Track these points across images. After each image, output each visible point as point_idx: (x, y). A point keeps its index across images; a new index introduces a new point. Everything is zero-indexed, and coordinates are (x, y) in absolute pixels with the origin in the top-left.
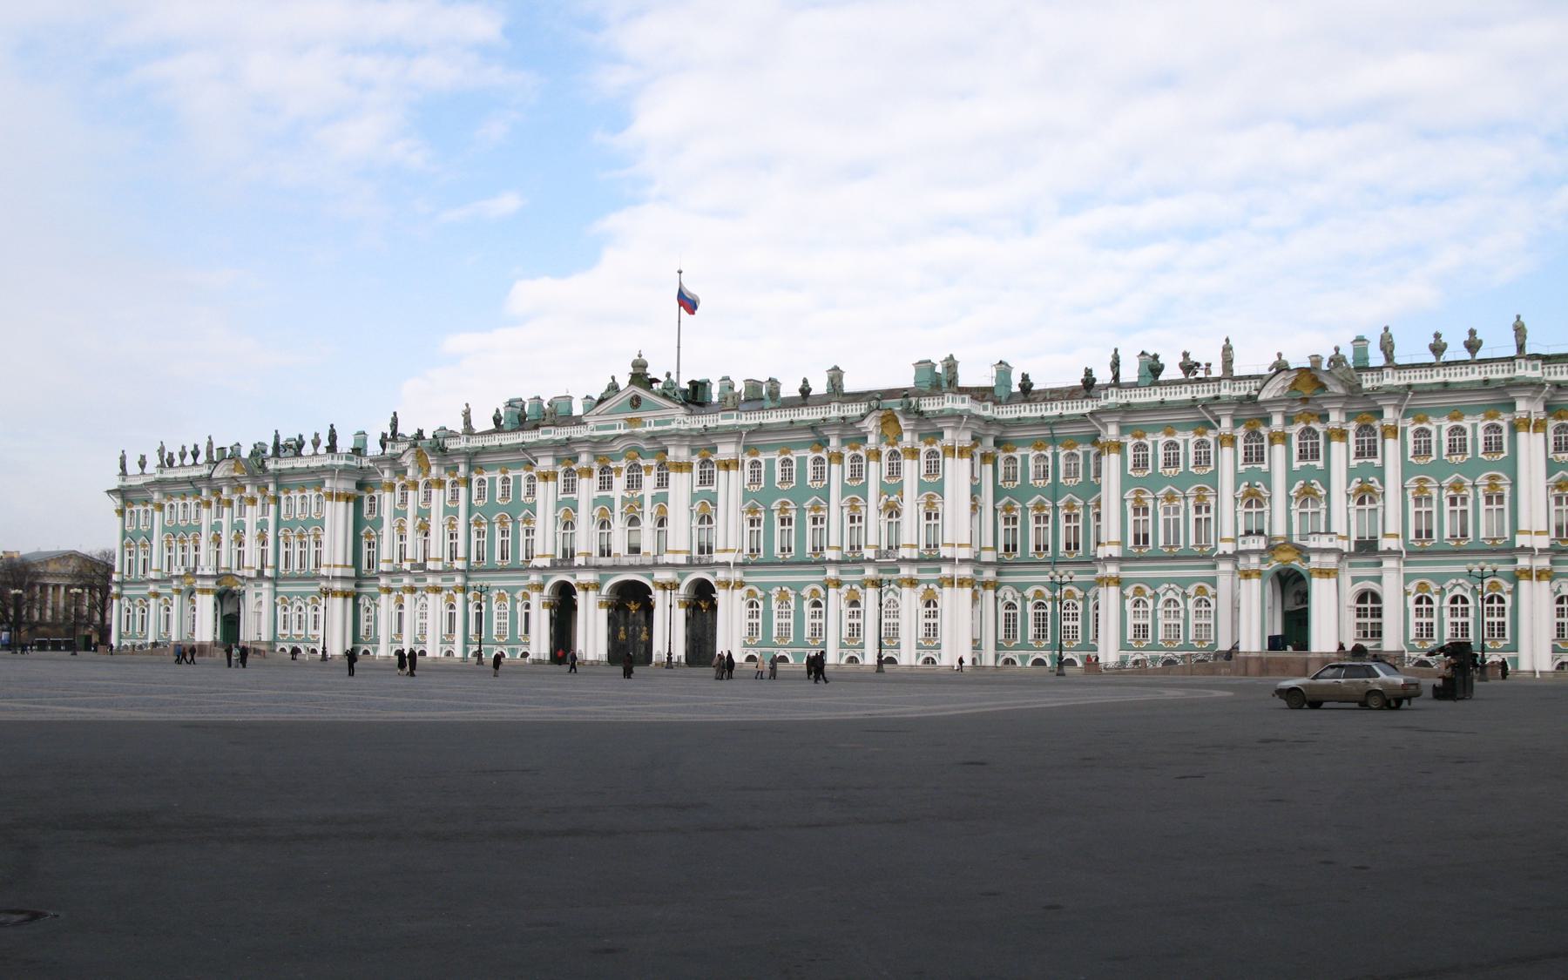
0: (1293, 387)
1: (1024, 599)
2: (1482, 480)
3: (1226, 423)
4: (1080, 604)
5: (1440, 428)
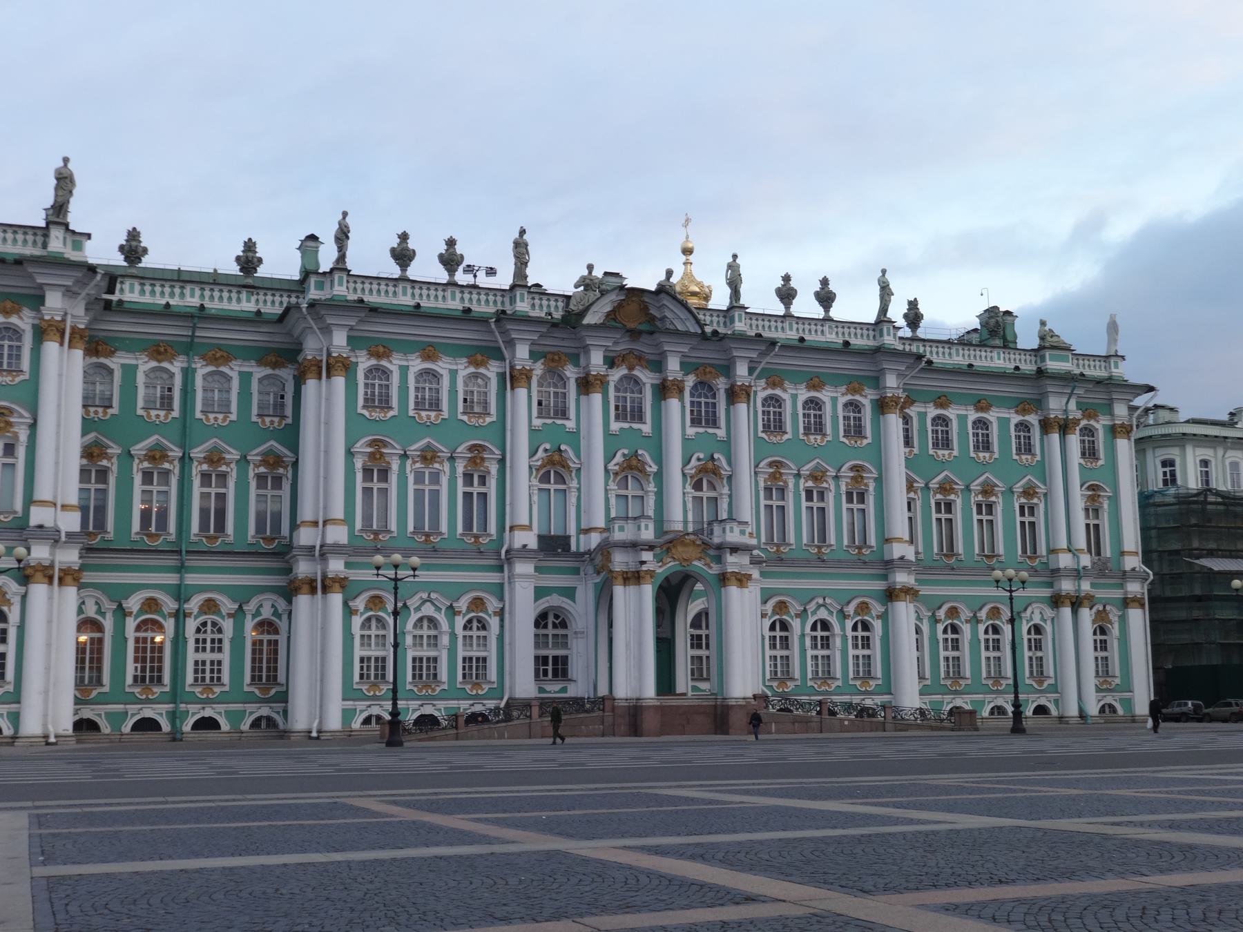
0: (612, 315)
1: (122, 613)
2: (845, 471)
3: (522, 352)
4: (228, 625)
5: (794, 396)
